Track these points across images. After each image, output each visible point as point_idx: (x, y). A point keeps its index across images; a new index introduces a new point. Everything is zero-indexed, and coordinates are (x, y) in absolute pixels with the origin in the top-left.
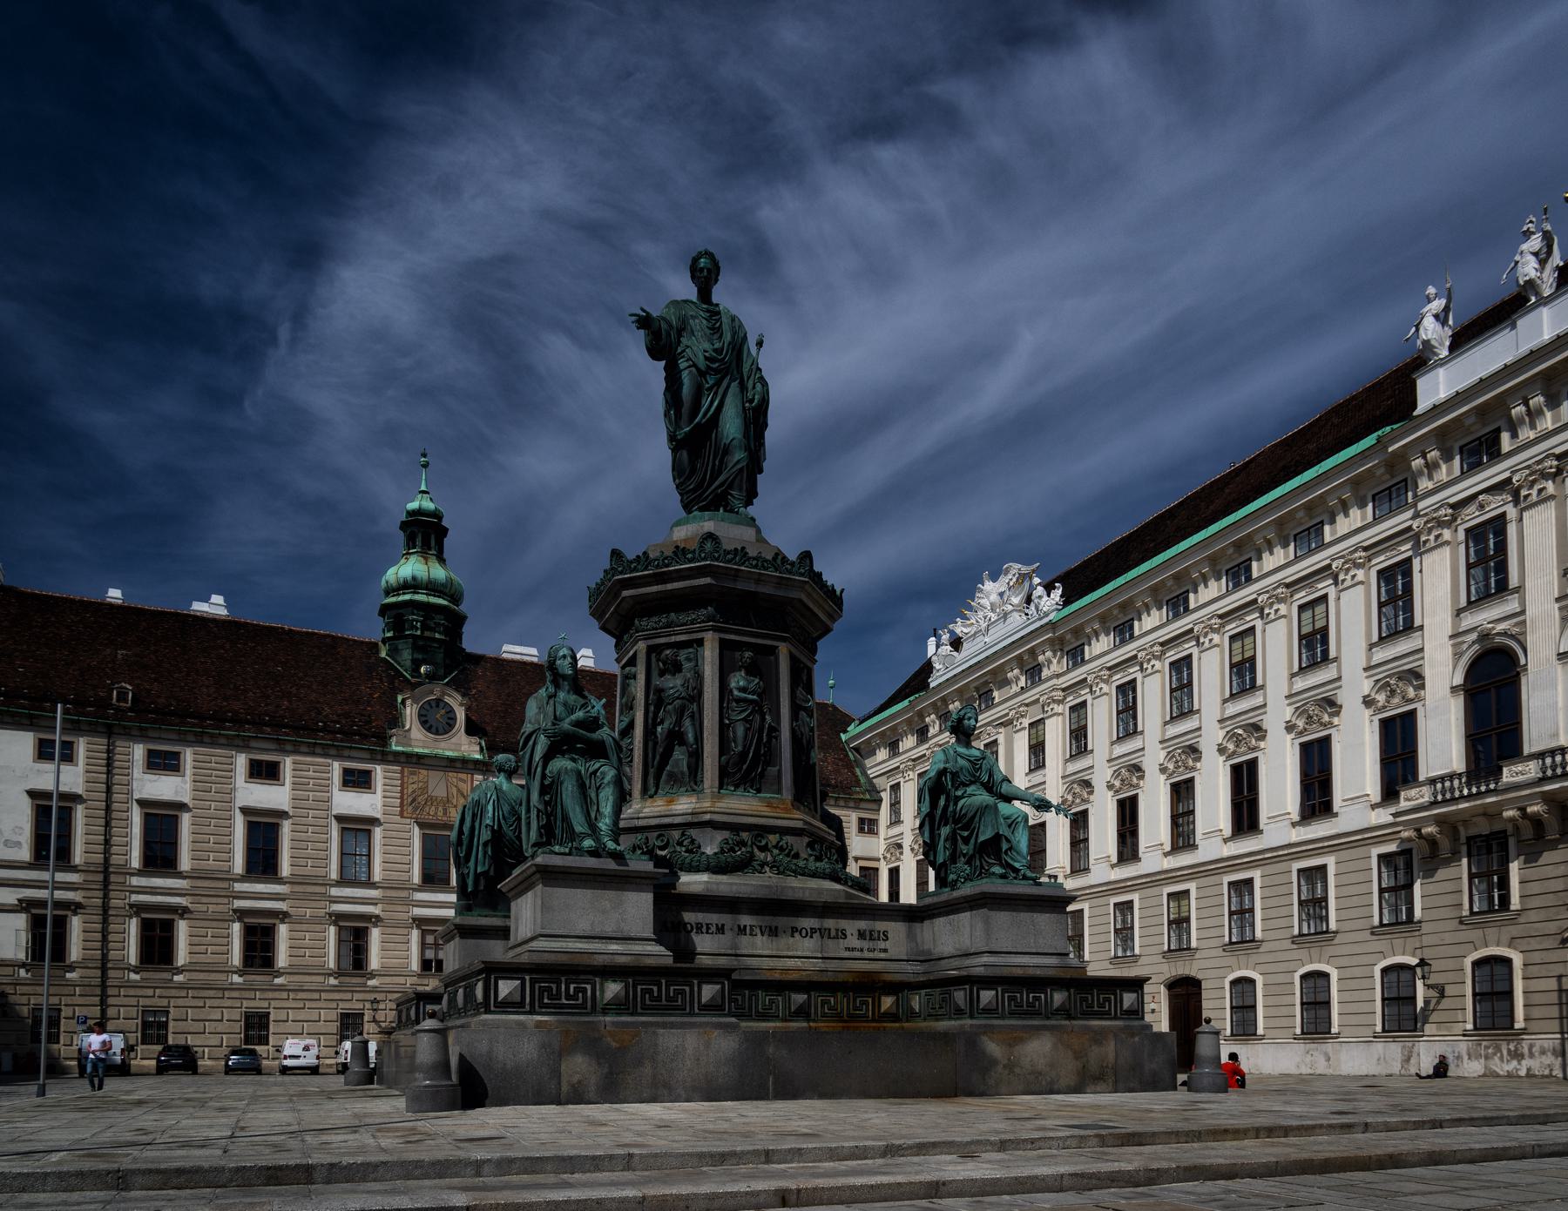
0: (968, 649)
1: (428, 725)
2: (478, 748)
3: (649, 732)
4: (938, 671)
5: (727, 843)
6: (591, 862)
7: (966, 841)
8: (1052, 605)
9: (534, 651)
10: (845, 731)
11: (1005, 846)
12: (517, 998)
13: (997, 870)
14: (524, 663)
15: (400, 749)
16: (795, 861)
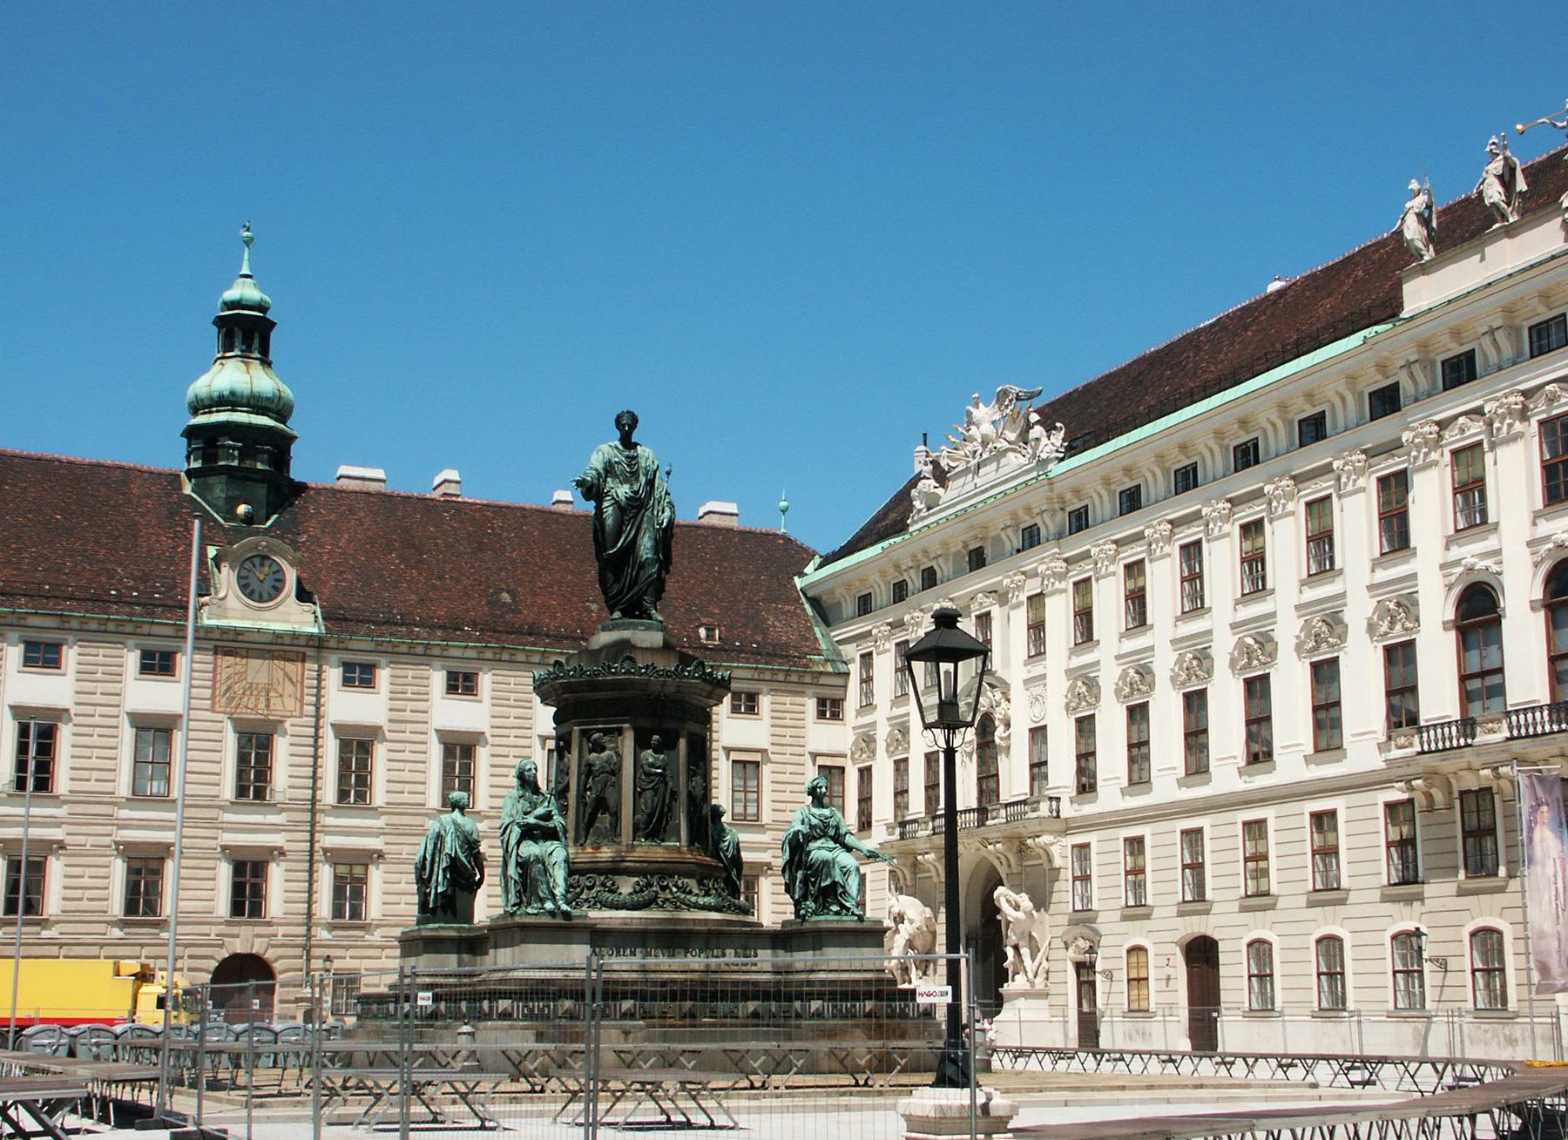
0: (955, 489)
1: (249, 590)
2: (312, 618)
3: (581, 796)
4: (920, 511)
5: (638, 884)
6: (547, 920)
7: (814, 884)
8: (1051, 452)
9: (382, 471)
10: (802, 575)
11: (840, 890)
12: (510, 1010)
13: (835, 908)
14: (368, 494)
15: (214, 622)
16: (688, 897)
